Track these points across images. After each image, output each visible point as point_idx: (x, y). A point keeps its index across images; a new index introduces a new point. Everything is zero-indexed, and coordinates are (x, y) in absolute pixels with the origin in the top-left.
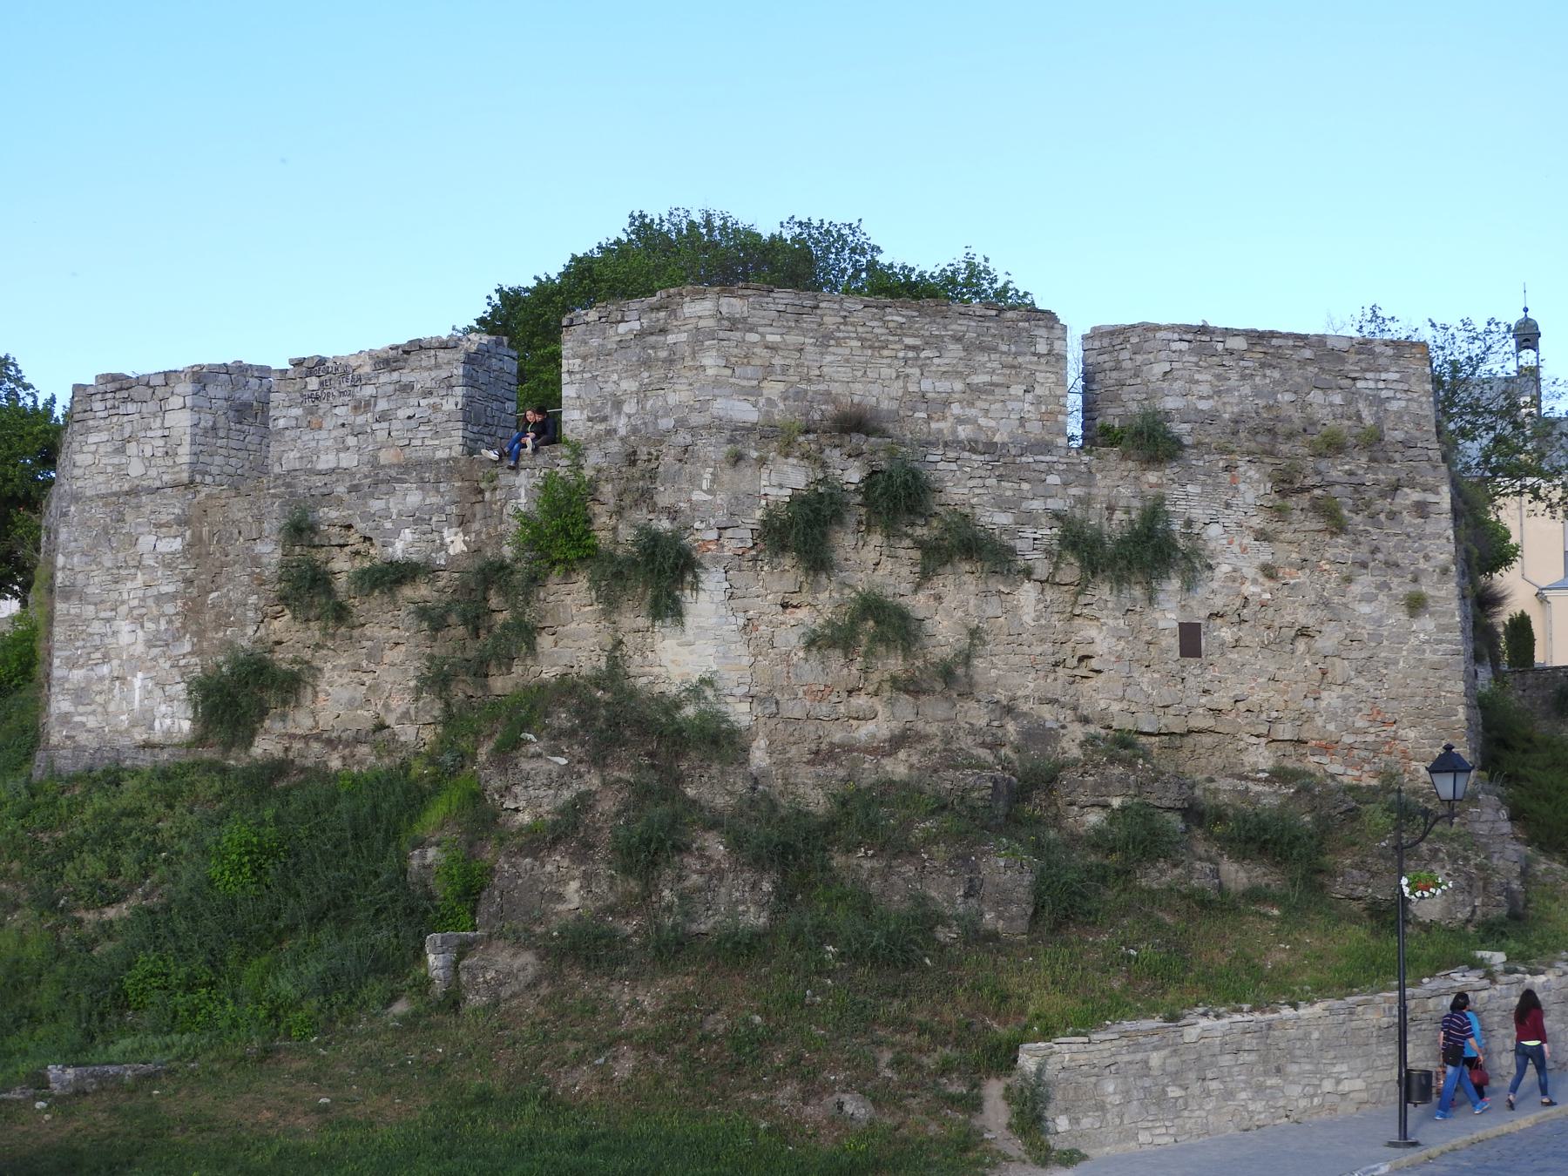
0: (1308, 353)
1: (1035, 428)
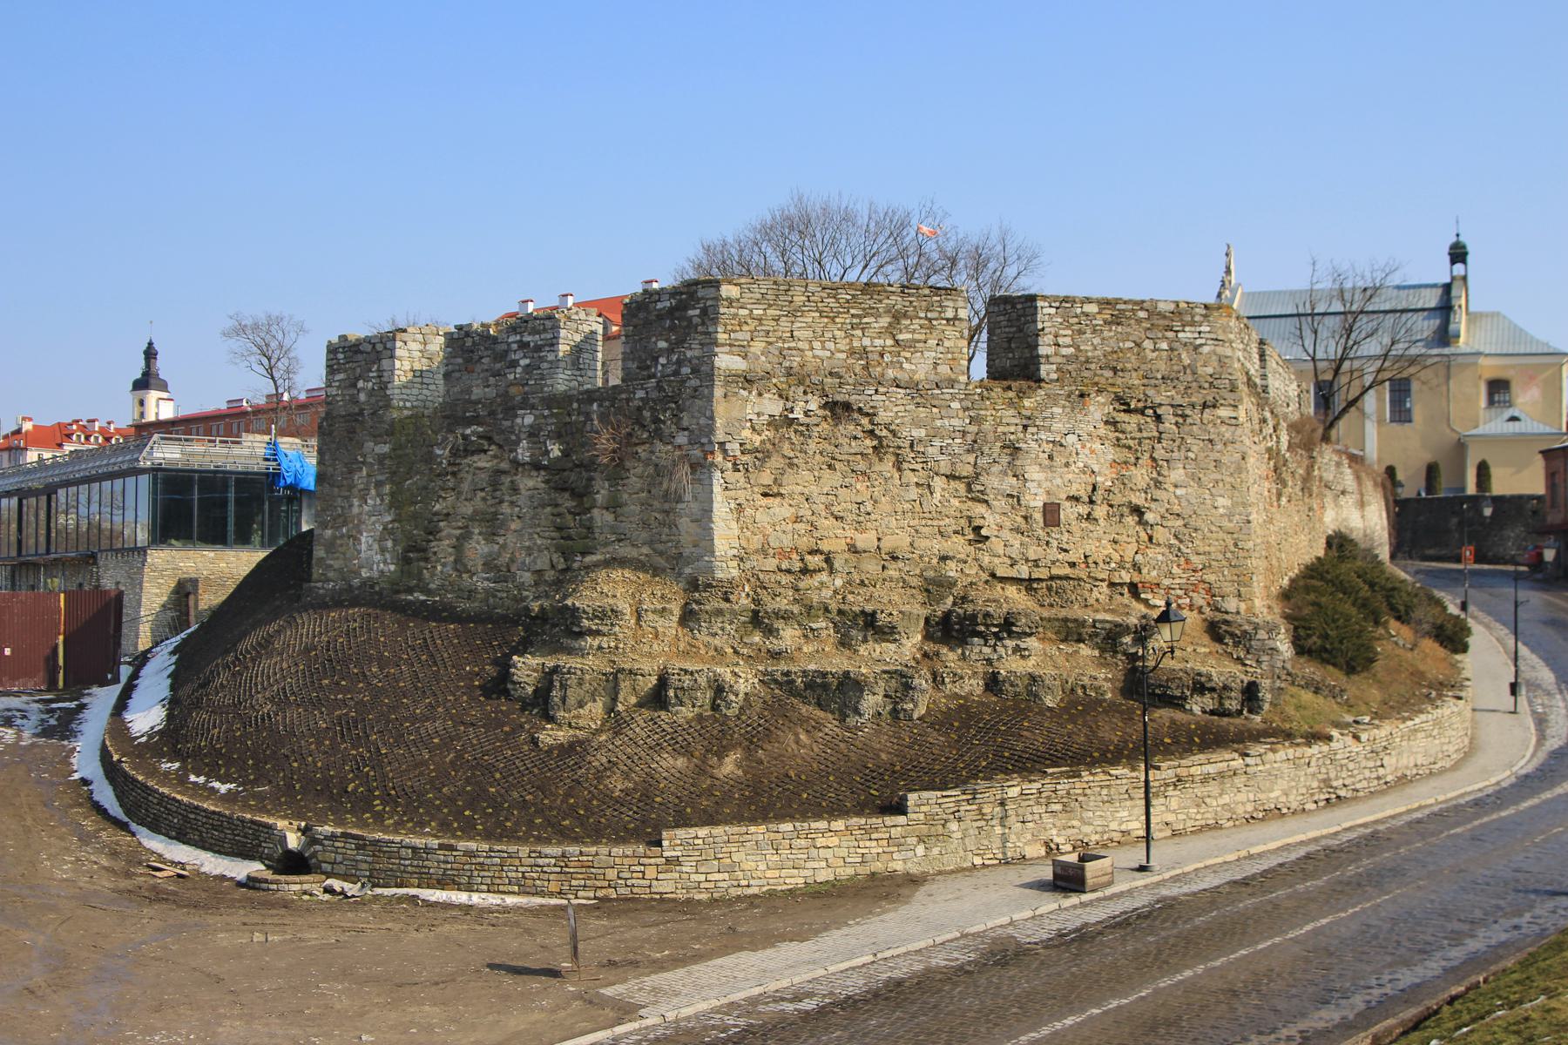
1: (944, 369)
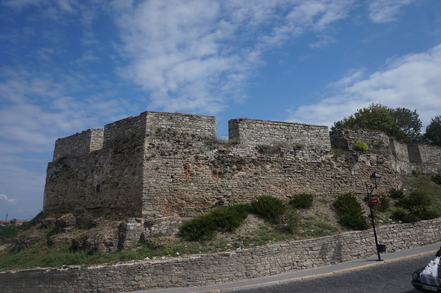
0: (125, 122)
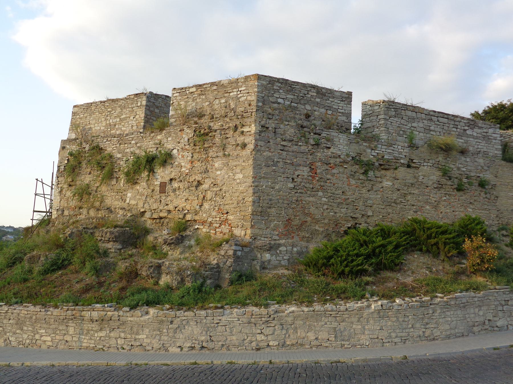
0: (215, 87)
